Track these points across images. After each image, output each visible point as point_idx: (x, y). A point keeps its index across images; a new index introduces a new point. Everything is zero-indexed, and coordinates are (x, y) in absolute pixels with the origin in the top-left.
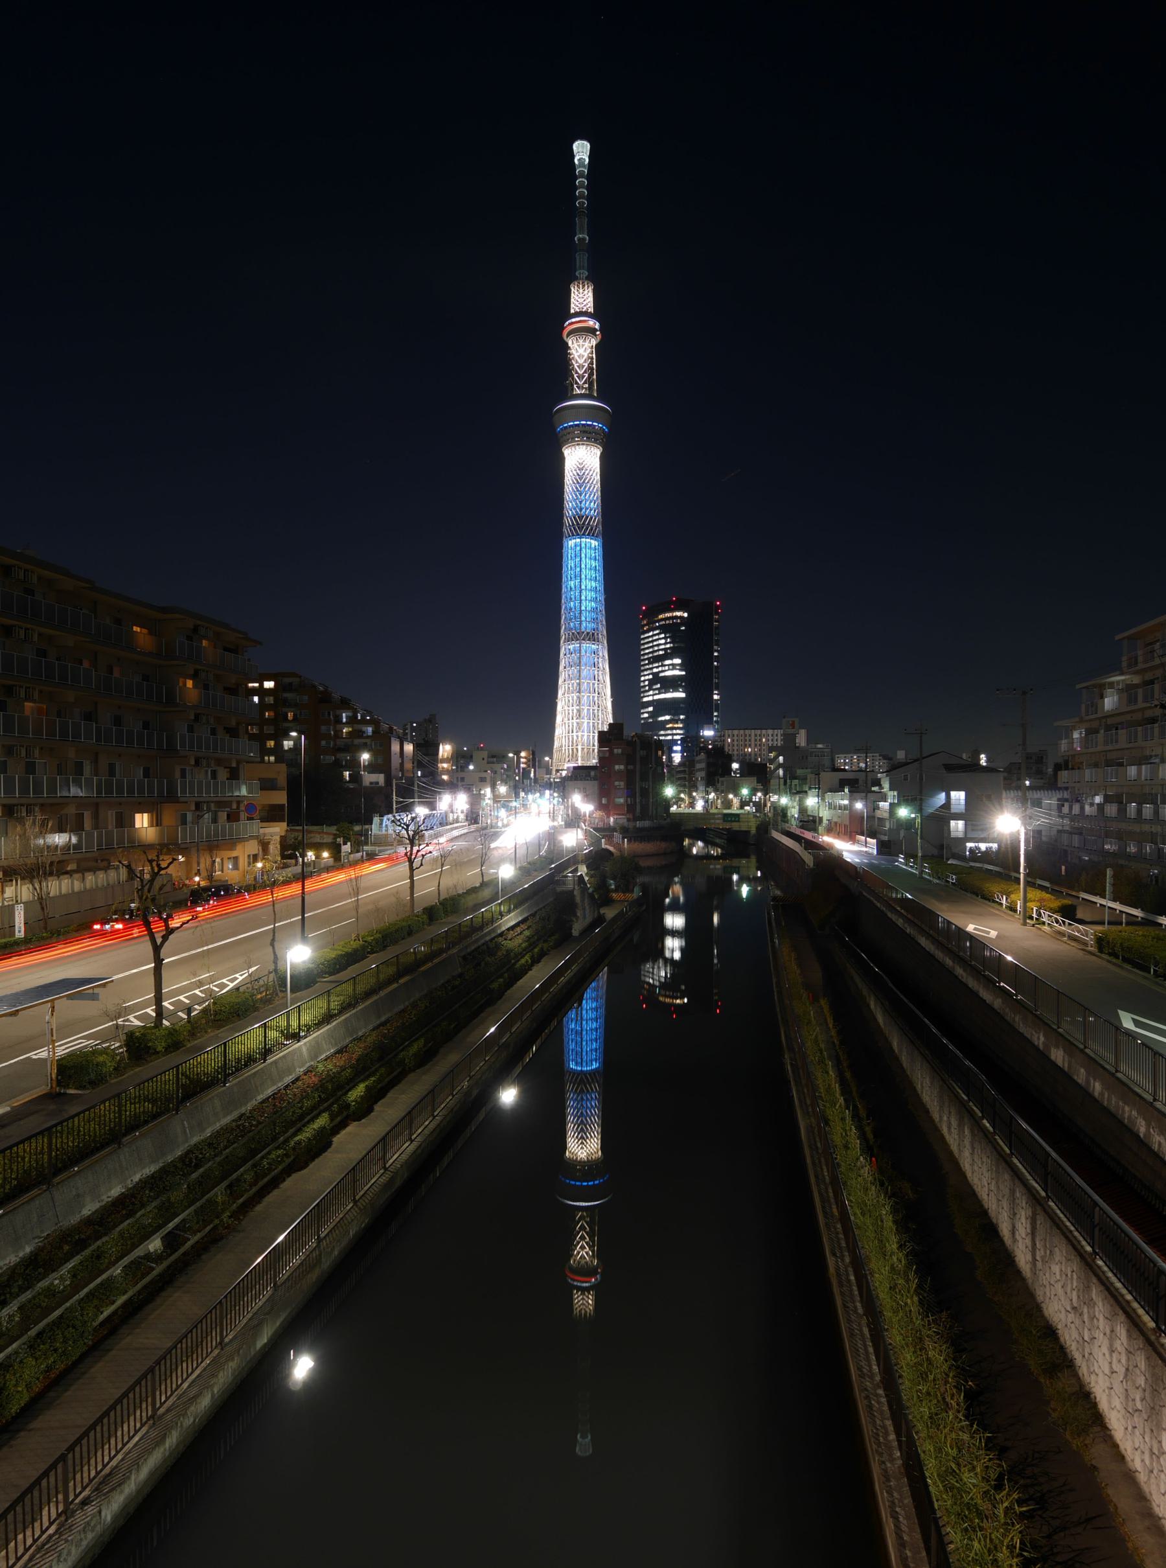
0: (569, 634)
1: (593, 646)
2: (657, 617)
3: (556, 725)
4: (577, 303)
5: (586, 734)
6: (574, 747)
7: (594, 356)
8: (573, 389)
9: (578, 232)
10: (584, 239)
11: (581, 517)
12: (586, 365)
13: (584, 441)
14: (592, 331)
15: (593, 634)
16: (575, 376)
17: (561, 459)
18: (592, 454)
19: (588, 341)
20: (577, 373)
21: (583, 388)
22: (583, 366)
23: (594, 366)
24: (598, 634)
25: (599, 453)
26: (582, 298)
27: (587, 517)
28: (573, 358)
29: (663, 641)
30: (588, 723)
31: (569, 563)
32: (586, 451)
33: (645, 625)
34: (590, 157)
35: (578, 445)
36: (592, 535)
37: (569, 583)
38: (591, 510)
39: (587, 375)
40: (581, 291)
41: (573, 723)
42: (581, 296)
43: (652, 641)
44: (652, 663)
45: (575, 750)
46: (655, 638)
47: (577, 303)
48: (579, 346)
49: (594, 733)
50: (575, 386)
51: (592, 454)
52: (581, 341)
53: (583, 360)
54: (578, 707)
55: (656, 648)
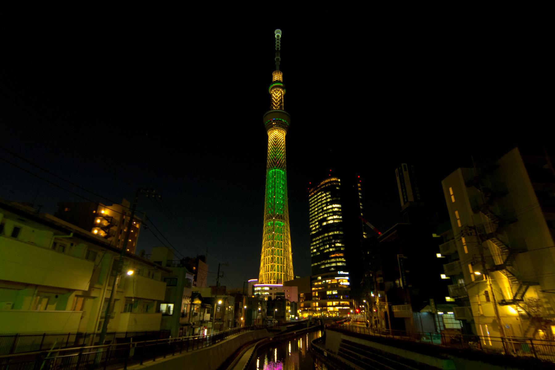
0: (268, 216)
1: (281, 222)
3: (260, 269)
5: (276, 272)
11: (275, 159)
12: (279, 99)
13: (278, 127)
14: (282, 88)
15: (281, 216)
16: (274, 104)
17: (267, 137)
21: (277, 107)
24: (284, 216)
26: (277, 77)
30: (278, 266)
31: (269, 182)
33: (311, 192)
35: (275, 129)
36: (281, 167)
37: (269, 191)
38: (280, 156)
39: (279, 103)
40: (277, 74)
41: (269, 266)
42: (276, 76)
43: (317, 200)
47: (275, 79)
48: (276, 93)
49: (281, 272)
50: (274, 107)
52: (277, 91)
54: (271, 256)
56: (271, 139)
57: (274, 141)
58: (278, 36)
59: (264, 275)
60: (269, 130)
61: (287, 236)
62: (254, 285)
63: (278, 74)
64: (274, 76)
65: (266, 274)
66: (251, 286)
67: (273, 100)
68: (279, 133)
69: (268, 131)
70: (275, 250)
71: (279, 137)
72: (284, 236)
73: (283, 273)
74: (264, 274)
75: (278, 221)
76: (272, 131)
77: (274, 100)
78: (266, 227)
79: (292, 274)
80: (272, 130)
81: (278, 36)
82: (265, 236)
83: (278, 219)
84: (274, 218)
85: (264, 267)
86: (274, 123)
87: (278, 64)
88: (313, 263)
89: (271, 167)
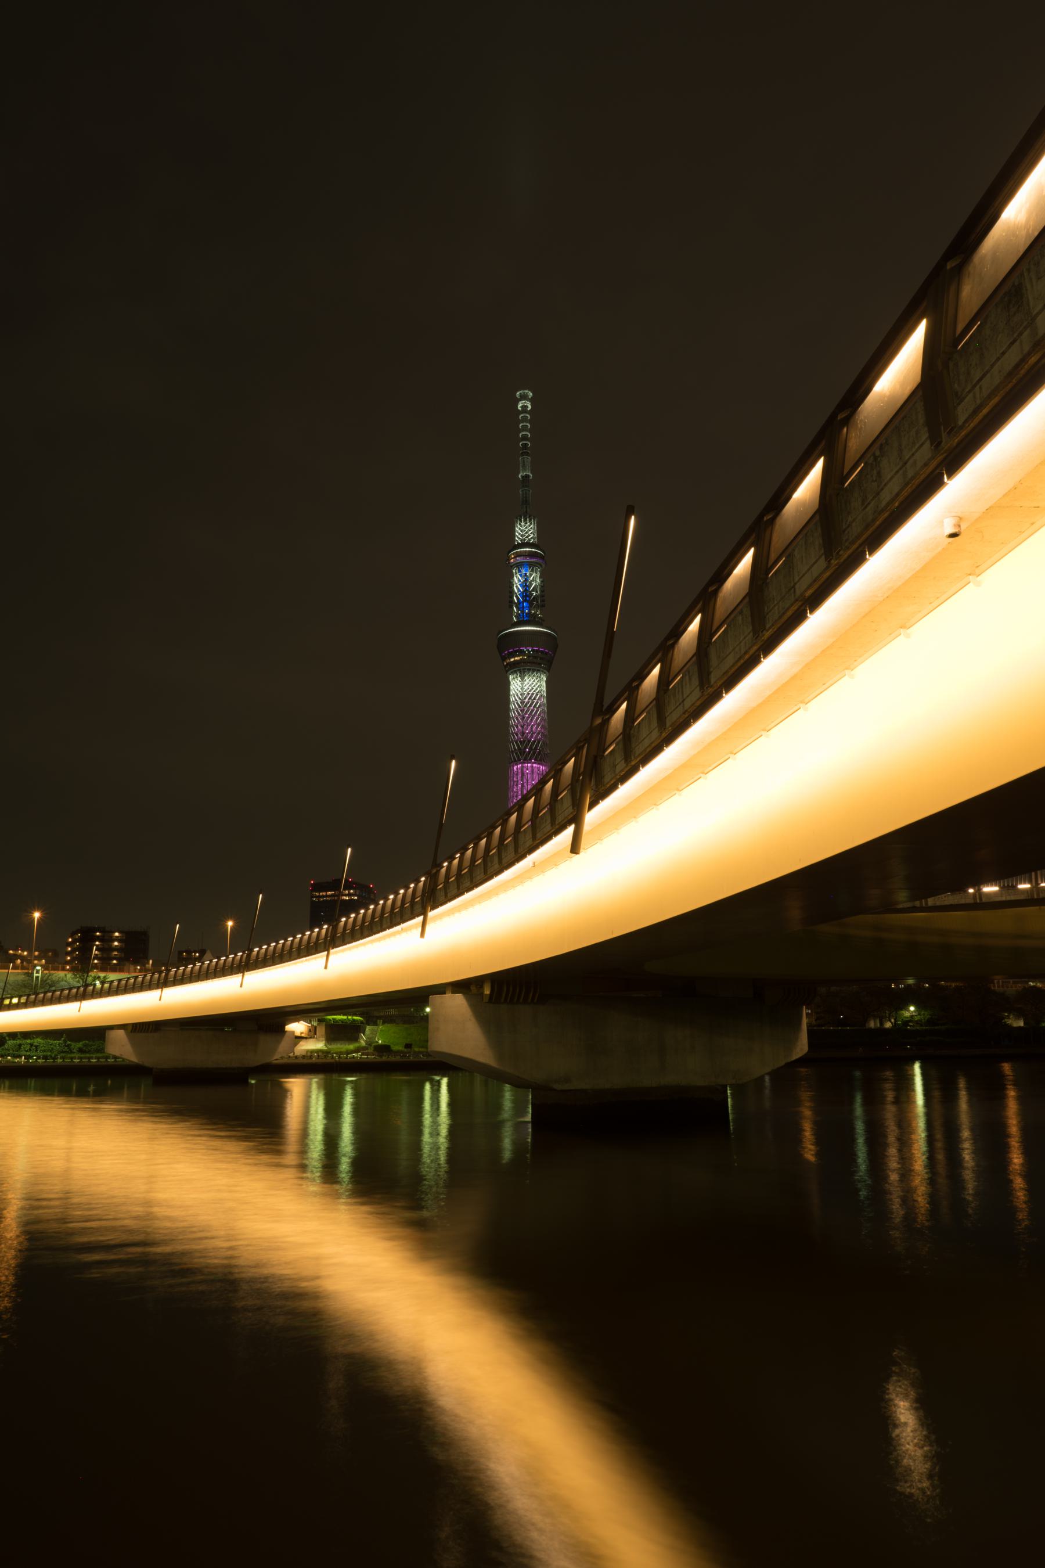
9: (521, 472)
10: (527, 476)
17: (509, 683)
27: (529, 741)
40: (523, 524)
48: (521, 575)
51: (535, 678)
56: (514, 693)
58: (524, 407)
60: (509, 672)
63: (526, 523)
68: (530, 678)
71: (530, 688)
81: (524, 407)
89: (515, 761)
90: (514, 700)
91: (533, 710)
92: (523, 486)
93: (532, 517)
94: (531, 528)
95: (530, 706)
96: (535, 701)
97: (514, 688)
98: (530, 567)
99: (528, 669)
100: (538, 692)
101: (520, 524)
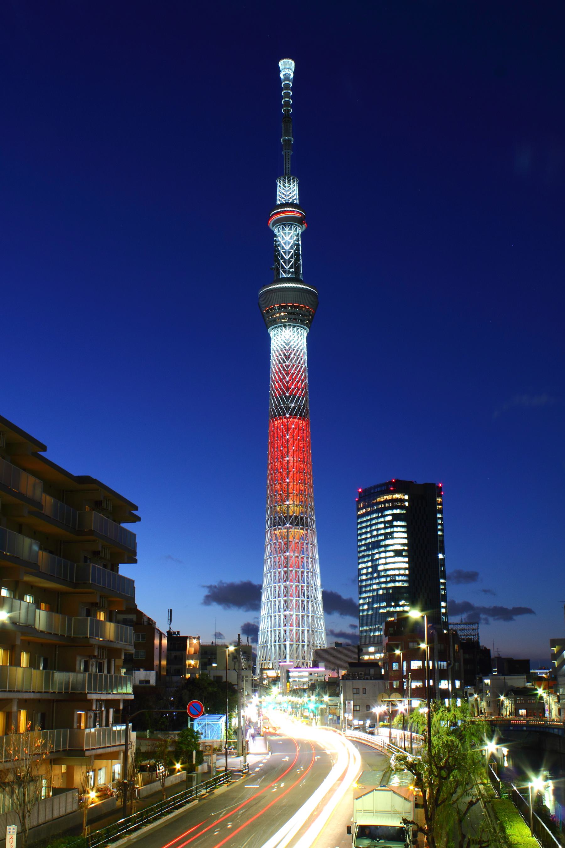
0: (275, 518)
1: (302, 531)
2: (376, 499)
4: (283, 196)
5: (294, 628)
6: (282, 643)
7: (300, 242)
8: (279, 273)
9: (283, 134)
10: (289, 140)
12: (293, 251)
14: (300, 221)
15: (302, 518)
16: (281, 261)
17: (269, 339)
18: (299, 335)
19: (293, 229)
20: (283, 258)
21: (289, 272)
22: (289, 252)
23: (300, 252)
24: (306, 518)
25: (305, 334)
28: (279, 245)
29: (382, 526)
32: (291, 333)
33: (361, 509)
34: (295, 73)
35: (285, 326)
39: (293, 260)
40: (287, 185)
44: (371, 549)
45: (282, 646)
46: (373, 522)
47: (283, 196)
48: (285, 234)
50: (281, 271)
51: (299, 335)
52: (287, 230)
53: (288, 248)
54: (285, 598)
55: (375, 533)
56: (278, 348)
57: (285, 355)
59: (271, 631)
60: (273, 327)
61: (313, 557)
62: (289, 670)
63: (290, 184)
64: (280, 186)
65: (275, 630)
66: (285, 671)
67: (280, 251)
69: (270, 329)
70: (292, 586)
71: (295, 344)
72: (307, 558)
73: (306, 629)
74: (269, 630)
75: (295, 528)
76: (279, 329)
77: (281, 251)
78: (271, 540)
79: (322, 629)
80: (279, 326)
82: (271, 558)
83: (296, 526)
84: (288, 525)
85: (271, 616)
86: (282, 314)
87: (287, 153)
88: (363, 627)
90: (278, 355)
91: (298, 366)
92: (286, 149)
93: (295, 179)
94: (294, 190)
95: (295, 361)
96: (300, 358)
97: (278, 343)
98: (294, 227)
99: (293, 326)
100: (302, 349)
101: (283, 185)
